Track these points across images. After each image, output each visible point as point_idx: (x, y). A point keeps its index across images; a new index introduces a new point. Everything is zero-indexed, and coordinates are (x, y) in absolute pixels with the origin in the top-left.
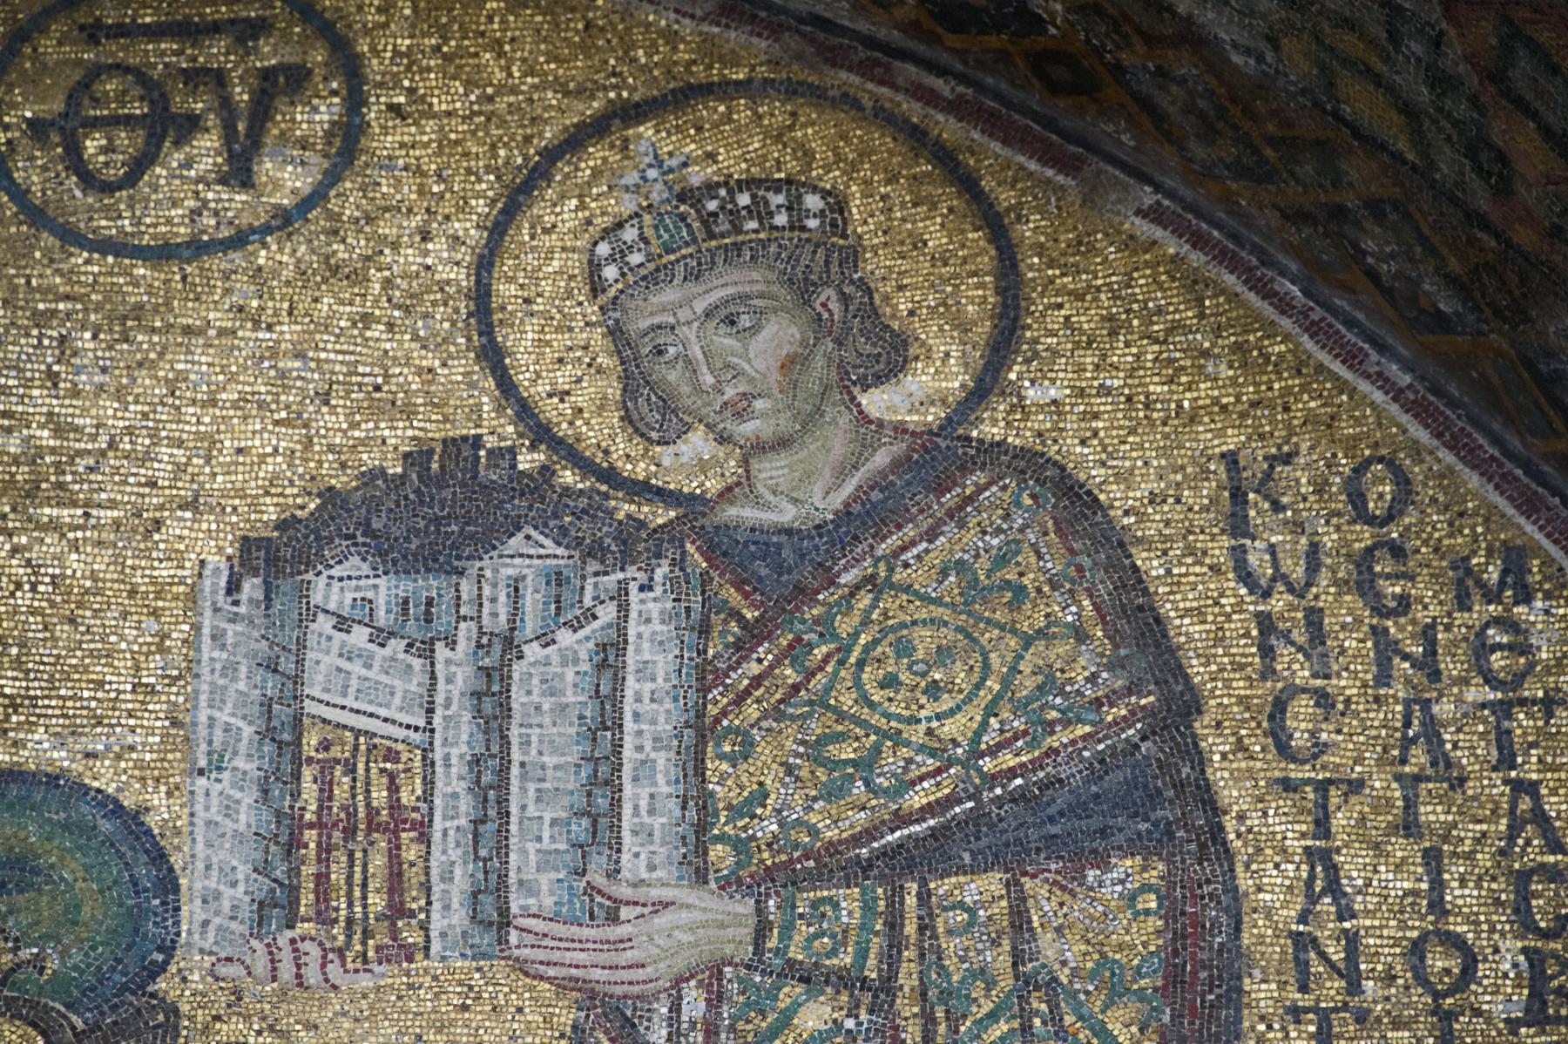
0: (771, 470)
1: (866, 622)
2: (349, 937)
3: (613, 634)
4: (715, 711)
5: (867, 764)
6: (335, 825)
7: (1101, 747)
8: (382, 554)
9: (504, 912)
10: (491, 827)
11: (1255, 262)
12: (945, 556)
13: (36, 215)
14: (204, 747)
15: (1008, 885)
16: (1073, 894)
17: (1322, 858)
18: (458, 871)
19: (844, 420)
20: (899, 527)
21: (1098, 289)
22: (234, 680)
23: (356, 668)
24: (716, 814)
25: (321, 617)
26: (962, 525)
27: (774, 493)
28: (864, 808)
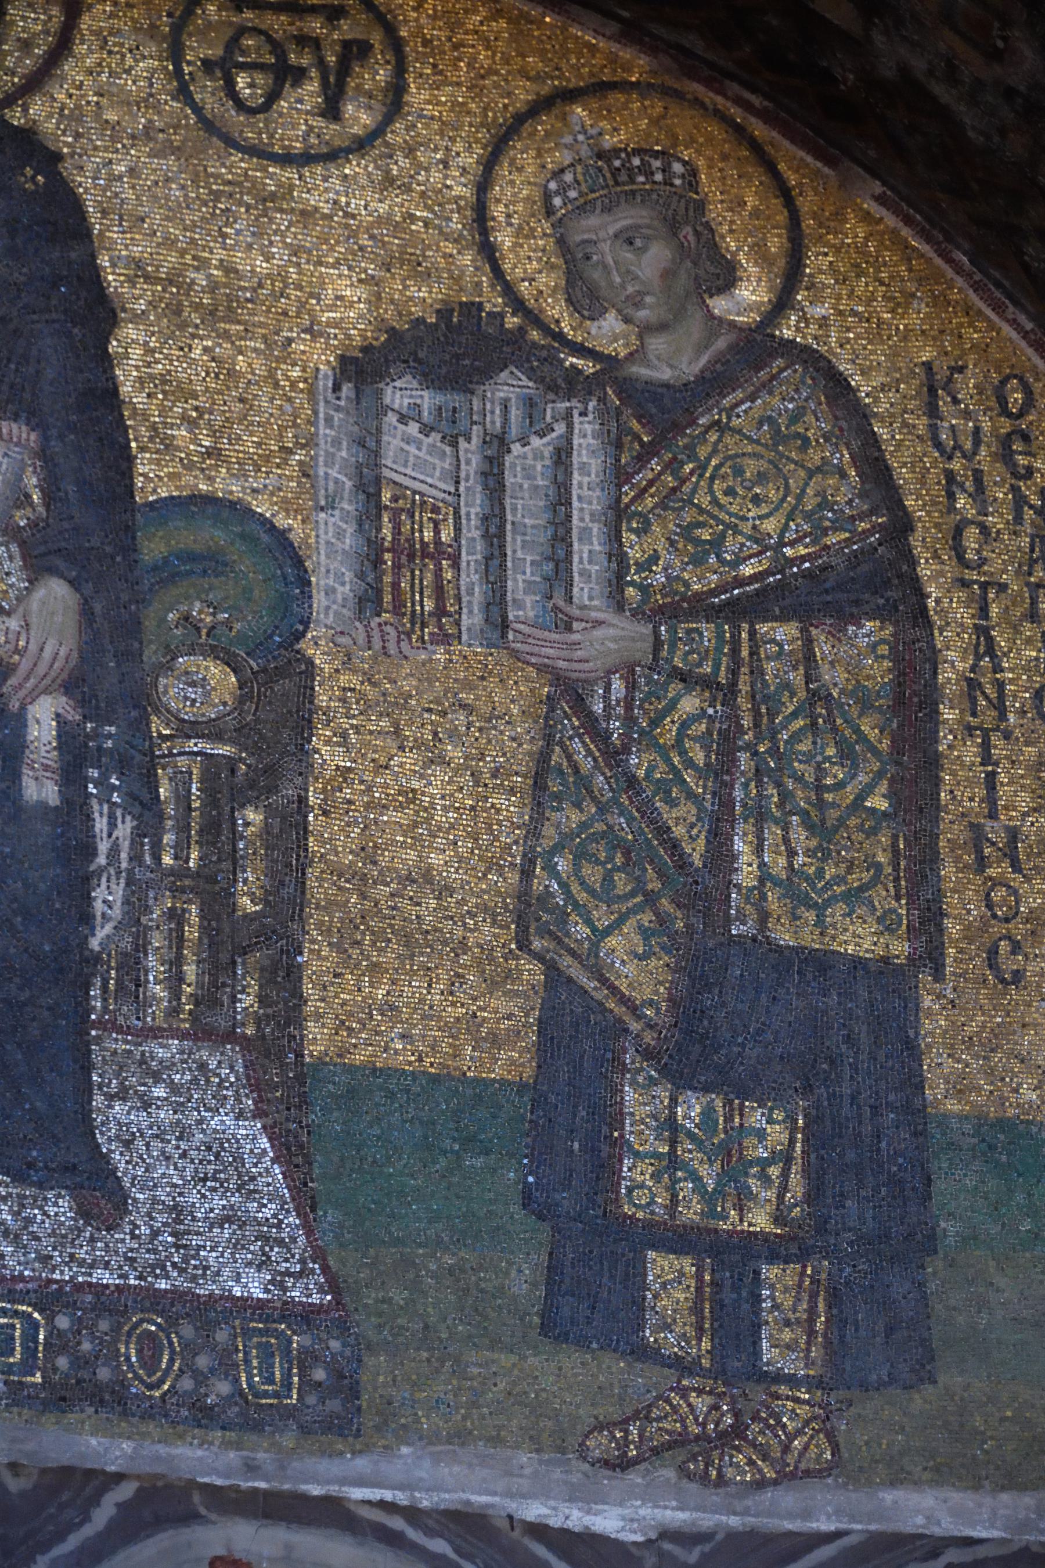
0: (657, 344)
1: (715, 452)
2: (413, 623)
3: (564, 440)
4: (626, 500)
5: (717, 543)
6: (402, 553)
7: (855, 547)
8: (425, 375)
9: (504, 618)
10: (496, 562)
11: (941, 238)
12: (761, 413)
13: (208, 125)
14: (323, 492)
15: (801, 631)
16: (840, 640)
17: (983, 631)
18: (477, 589)
19: (699, 315)
20: (734, 390)
21: (849, 245)
22: (339, 450)
23: (412, 449)
24: (629, 567)
25: (390, 413)
26: (771, 393)
27: (658, 359)
28: (715, 573)
